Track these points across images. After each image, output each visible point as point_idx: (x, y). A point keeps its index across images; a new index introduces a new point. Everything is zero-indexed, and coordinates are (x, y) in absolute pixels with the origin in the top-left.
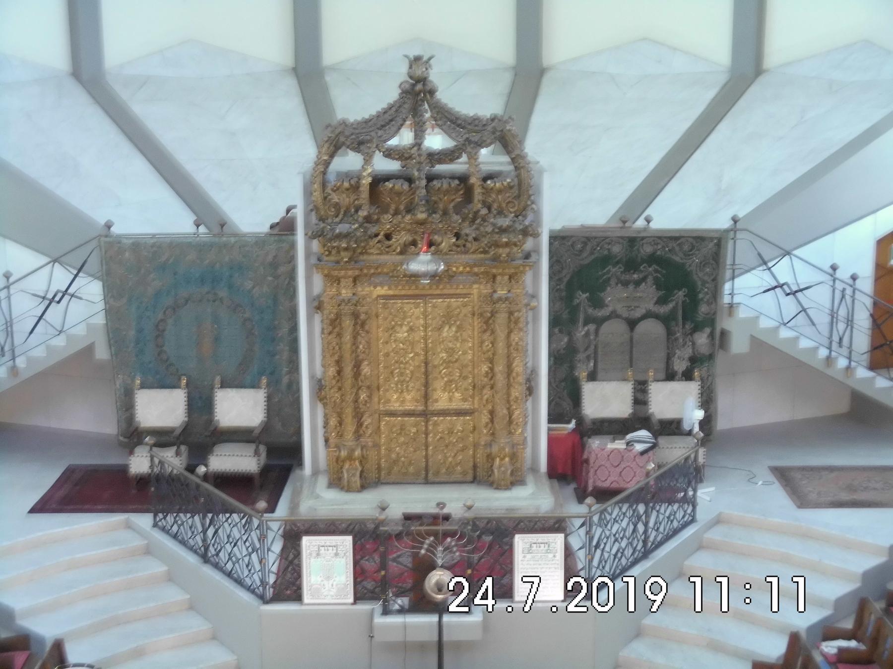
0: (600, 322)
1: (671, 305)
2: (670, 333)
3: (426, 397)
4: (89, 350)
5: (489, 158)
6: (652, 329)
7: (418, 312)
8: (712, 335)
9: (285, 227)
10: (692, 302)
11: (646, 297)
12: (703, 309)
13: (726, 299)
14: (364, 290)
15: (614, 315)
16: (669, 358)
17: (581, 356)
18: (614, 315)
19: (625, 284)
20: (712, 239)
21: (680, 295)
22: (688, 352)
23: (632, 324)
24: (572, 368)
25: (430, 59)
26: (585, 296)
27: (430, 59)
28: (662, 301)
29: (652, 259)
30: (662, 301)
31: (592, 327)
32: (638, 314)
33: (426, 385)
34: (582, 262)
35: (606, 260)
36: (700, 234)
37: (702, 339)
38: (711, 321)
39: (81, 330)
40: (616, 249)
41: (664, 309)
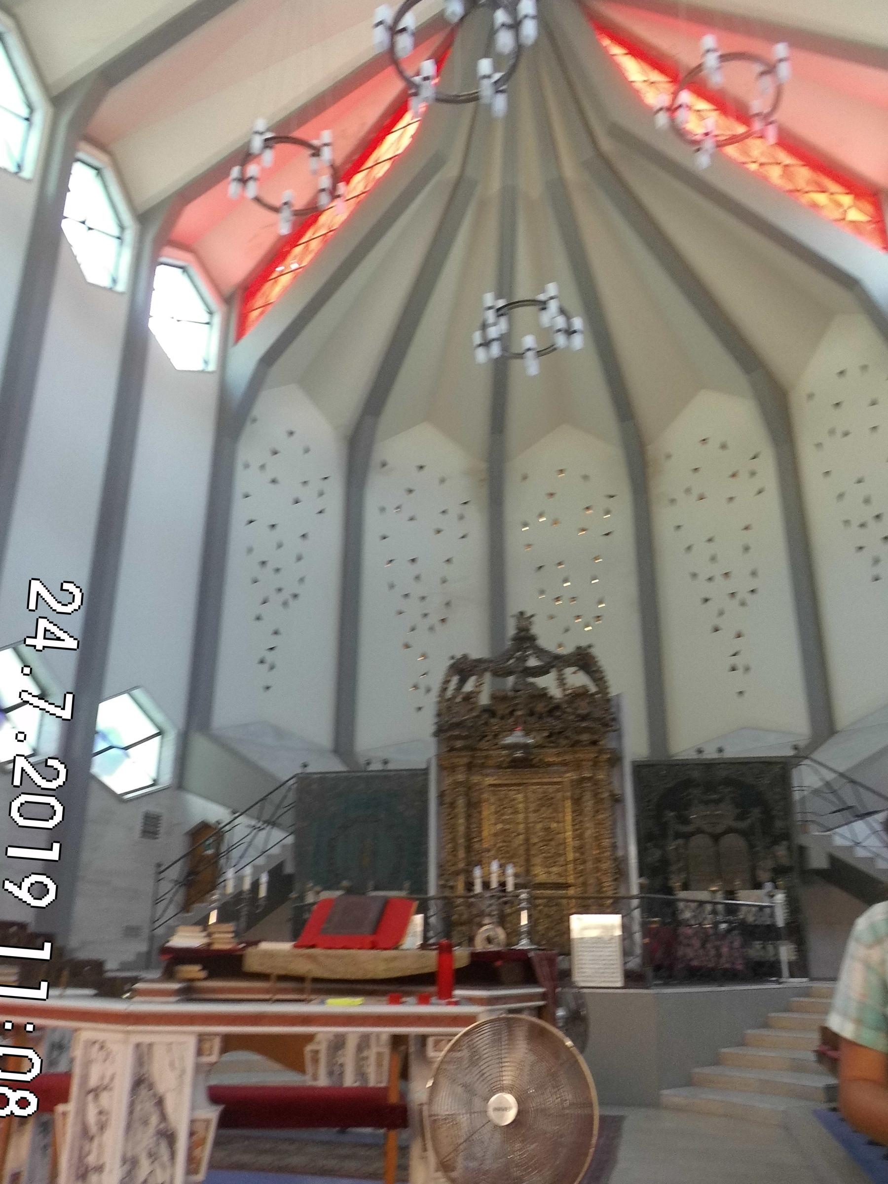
0: (687, 836)
1: (749, 821)
2: (752, 846)
3: (528, 872)
4: (280, 866)
5: (577, 679)
6: (734, 842)
7: (520, 797)
8: (789, 848)
9: (429, 762)
10: (768, 819)
11: (726, 814)
12: (779, 824)
13: (799, 817)
14: (475, 779)
15: (699, 831)
16: (753, 869)
17: (674, 868)
18: (699, 831)
19: (707, 803)
20: (776, 763)
21: (756, 812)
22: (770, 864)
23: (716, 838)
24: (667, 879)
25: (532, 616)
26: (672, 814)
27: (532, 616)
28: (741, 817)
29: (728, 782)
30: (741, 817)
31: (680, 841)
32: (719, 829)
33: (528, 860)
34: (668, 786)
35: (688, 783)
36: (767, 760)
37: (781, 851)
38: (786, 836)
39: (275, 851)
40: (696, 774)
41: (743, 825)
